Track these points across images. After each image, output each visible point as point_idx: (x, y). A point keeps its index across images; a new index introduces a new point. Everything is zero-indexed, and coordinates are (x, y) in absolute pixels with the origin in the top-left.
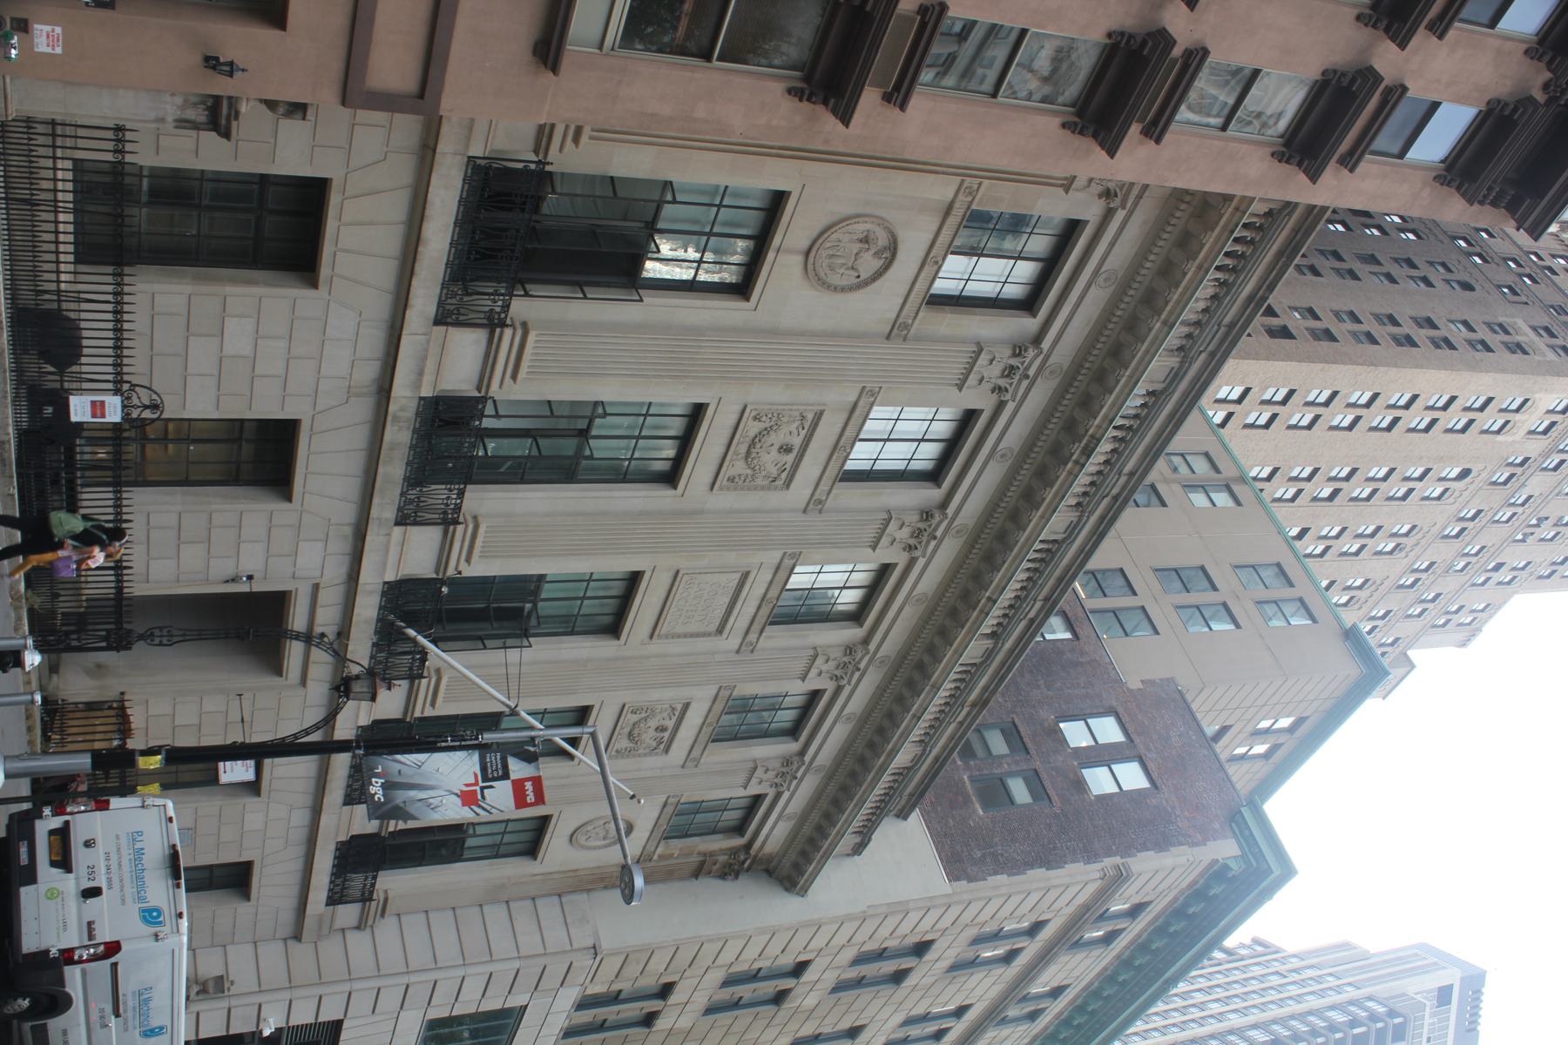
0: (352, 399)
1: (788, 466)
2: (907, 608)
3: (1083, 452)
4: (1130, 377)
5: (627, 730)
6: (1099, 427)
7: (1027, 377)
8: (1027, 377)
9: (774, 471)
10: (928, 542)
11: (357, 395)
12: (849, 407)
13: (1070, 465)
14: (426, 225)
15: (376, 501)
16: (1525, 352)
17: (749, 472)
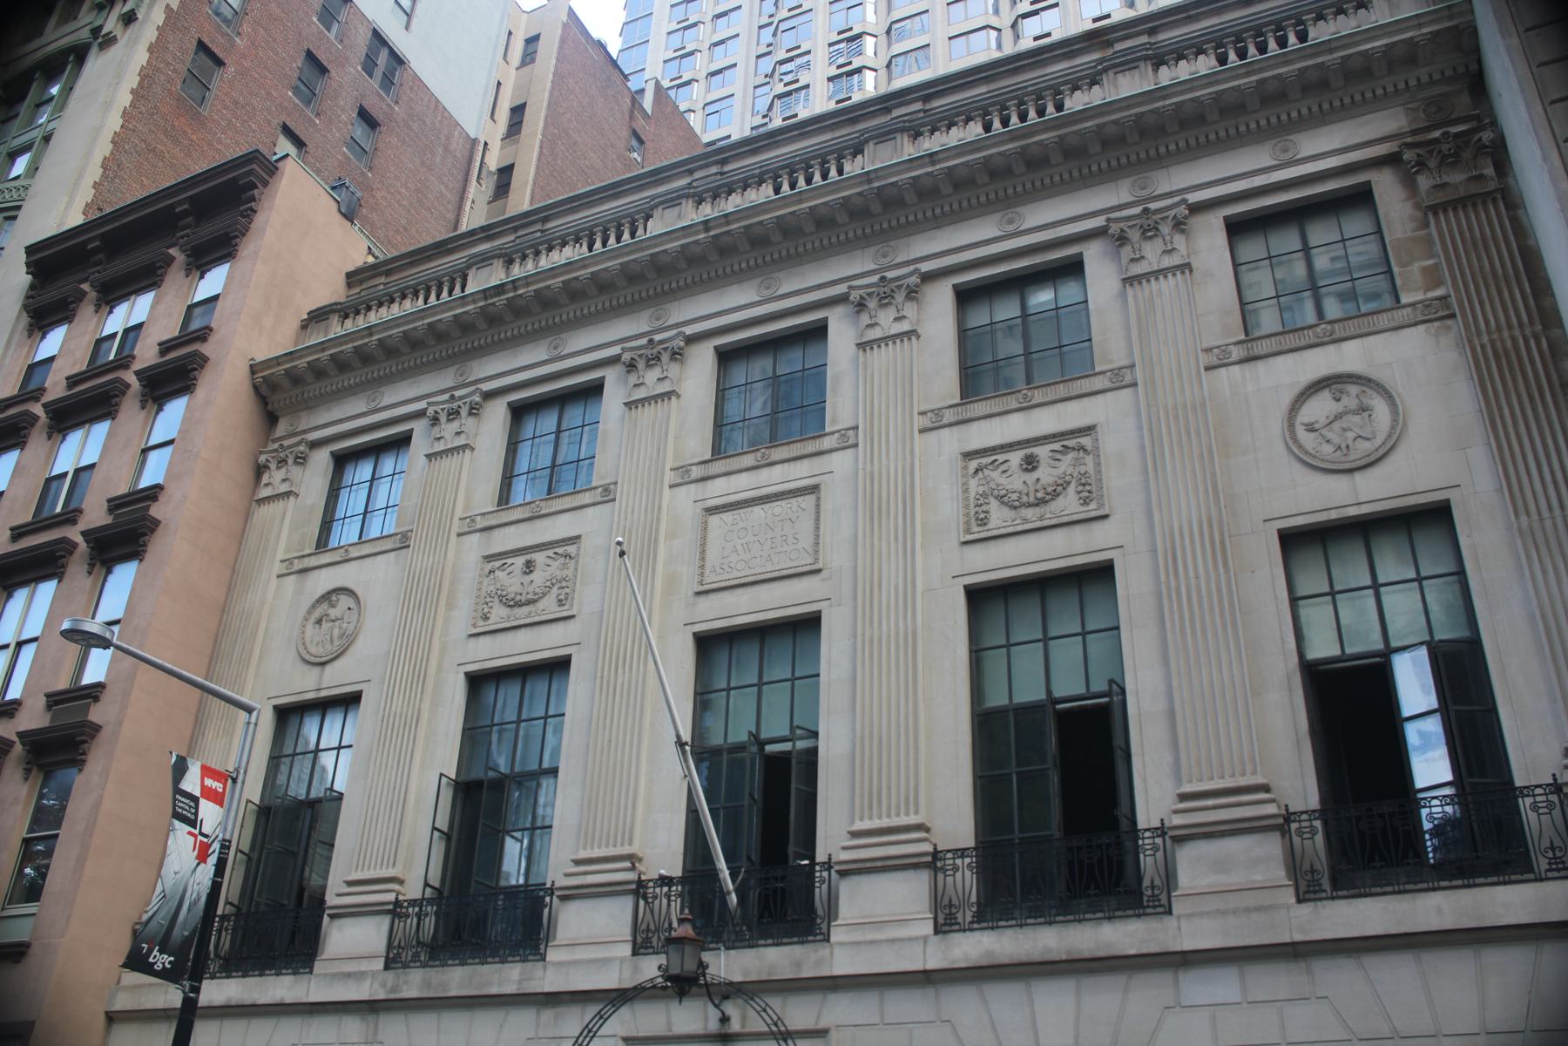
0: (379, 1038)
1: (550, 553)
2: (899, 259)
3: (504, 292)
4: (422, 318)
5: (1030, 513)
6: (474, 302)
7: (452, 397)
8: (452, 397)
9: (556, 564)
10: (661, 342)
11: (376, 1033)
12: (485, 534)
13: (520, 292)
14: (216, 1003)
15: (494, 990)
16: (407, 28)
17: (555, 590)
